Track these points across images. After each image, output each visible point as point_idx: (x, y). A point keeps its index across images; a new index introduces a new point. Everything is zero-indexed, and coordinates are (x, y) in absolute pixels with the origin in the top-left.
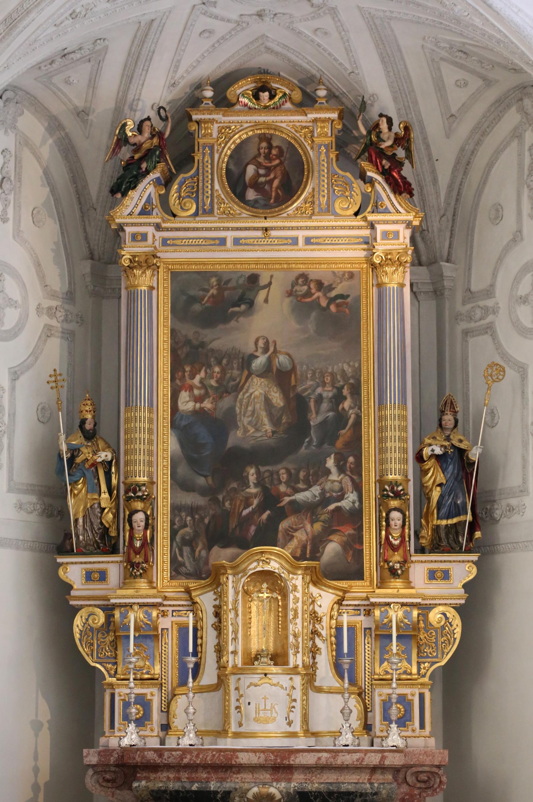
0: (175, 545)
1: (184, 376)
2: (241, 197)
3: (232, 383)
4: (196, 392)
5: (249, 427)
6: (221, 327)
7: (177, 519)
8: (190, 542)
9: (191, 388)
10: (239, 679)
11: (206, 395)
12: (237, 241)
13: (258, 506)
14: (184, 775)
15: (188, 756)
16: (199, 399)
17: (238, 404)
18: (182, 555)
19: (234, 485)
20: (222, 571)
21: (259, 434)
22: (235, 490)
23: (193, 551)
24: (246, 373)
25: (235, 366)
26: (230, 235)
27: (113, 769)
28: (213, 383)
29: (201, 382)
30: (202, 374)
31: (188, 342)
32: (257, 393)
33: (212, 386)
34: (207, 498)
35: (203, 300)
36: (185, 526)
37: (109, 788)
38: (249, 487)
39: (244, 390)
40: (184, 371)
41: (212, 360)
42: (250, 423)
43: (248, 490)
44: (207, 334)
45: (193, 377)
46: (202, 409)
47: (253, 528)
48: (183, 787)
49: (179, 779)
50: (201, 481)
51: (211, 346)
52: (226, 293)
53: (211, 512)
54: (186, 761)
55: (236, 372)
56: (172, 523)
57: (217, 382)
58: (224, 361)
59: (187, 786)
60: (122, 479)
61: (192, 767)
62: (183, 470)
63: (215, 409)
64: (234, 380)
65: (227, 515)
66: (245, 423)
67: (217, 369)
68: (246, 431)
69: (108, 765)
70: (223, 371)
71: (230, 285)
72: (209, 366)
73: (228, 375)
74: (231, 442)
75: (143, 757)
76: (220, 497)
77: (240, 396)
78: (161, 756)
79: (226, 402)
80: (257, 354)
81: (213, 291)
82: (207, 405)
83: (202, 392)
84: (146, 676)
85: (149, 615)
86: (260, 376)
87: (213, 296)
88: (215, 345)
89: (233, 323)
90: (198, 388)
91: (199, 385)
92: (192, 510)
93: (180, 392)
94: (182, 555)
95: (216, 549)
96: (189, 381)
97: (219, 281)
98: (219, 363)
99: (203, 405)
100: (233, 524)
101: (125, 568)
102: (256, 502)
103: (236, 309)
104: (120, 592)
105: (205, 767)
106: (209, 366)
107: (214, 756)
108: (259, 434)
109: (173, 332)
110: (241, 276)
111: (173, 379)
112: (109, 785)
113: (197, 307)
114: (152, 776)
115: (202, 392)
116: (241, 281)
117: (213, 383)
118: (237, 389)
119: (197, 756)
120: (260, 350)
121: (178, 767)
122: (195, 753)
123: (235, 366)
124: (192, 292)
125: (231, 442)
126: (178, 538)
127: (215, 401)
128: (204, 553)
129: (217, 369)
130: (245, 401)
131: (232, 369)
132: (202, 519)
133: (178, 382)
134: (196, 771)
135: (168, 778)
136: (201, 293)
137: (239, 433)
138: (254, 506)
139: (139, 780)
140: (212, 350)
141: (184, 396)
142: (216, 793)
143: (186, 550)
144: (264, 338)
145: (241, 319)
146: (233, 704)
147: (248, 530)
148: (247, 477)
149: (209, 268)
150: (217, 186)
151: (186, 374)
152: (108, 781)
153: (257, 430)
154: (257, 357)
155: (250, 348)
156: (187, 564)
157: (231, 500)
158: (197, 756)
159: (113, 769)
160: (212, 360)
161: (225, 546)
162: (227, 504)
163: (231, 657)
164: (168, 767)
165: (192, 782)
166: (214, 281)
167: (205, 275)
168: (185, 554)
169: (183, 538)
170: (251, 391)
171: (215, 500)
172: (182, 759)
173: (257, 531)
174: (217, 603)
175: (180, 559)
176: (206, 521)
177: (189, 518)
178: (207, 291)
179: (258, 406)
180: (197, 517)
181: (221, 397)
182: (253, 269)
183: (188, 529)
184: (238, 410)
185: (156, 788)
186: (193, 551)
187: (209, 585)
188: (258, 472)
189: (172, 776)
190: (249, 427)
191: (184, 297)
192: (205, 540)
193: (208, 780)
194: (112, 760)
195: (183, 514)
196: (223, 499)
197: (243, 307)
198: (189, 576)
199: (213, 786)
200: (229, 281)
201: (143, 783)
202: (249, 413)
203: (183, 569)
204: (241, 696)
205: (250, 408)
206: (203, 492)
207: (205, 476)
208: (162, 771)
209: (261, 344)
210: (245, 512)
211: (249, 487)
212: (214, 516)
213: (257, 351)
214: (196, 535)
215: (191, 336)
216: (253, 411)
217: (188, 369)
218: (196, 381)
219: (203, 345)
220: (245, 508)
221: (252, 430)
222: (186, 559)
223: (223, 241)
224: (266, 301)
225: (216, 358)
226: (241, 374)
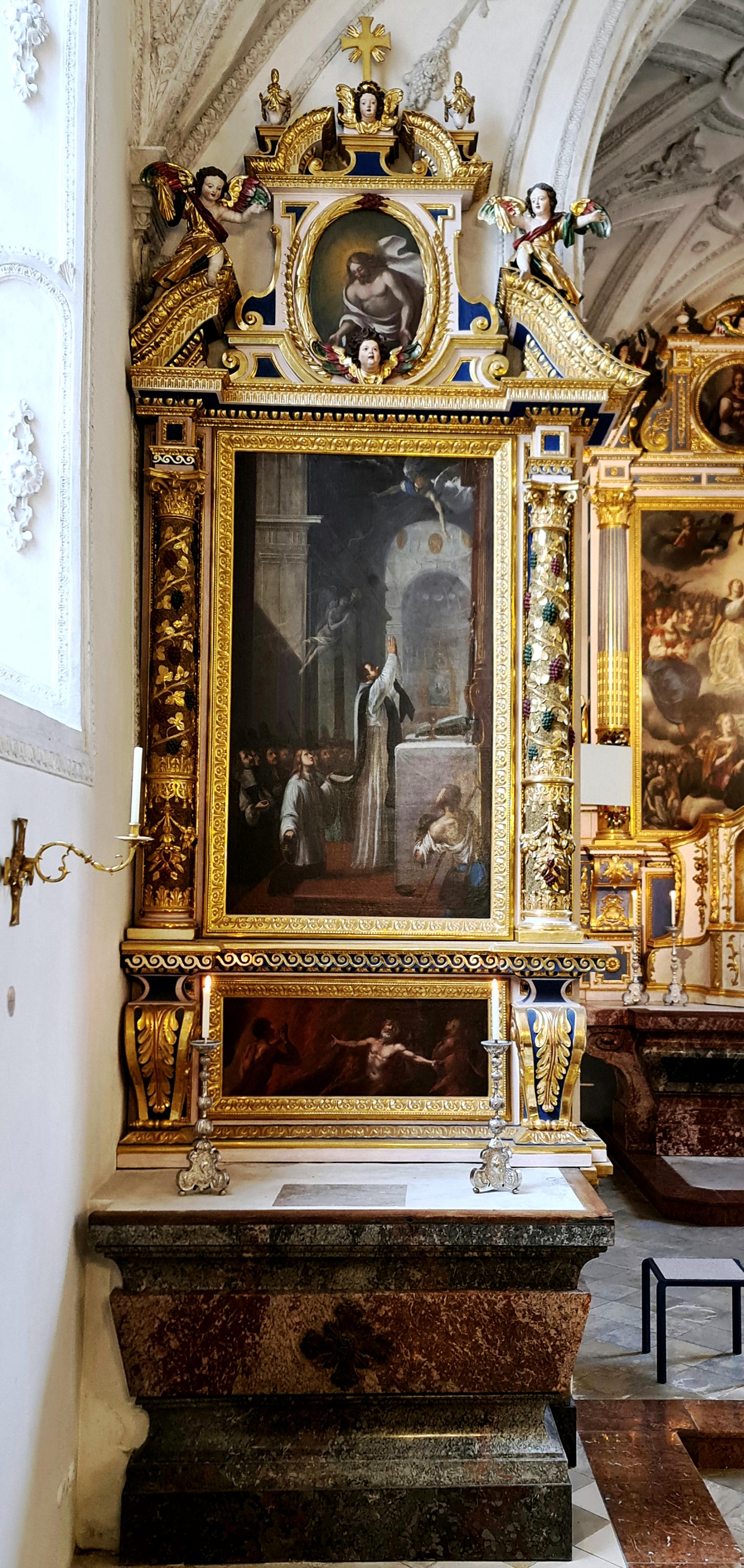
0: (646, 794)
1: (655, 620)
2: (714, 433)
3: (705, 628)
4: (668, 637)
5: (723, 674)
6: (694, 569)
7: (649, 768)
8: (662, 792)
9: (662, 633)
10: (733, 936)
11: (679, 640)
12: (711, 479)
13: (732, 755)
14: (697, 1042)
15: (705, 1023)
16: (671, 645)
17: (711, 651)
18: (654, 805)
19: (708, 733)
20: (711, 823)
21: (731, 682)
22: (707, 738)
23: (665, 801)
24: (719, 618)
25: (708, 610)
26: (704, 472)
27: (611, 1030)
28: (685, 627)
29: (673, 626)
30: (674, 618)
31: (660, 585)
32: (730, 639)
33: (684, 632)
34: (679, 747)
35: (674, 540)
36: (657, 775)
37: (606, 1050)
38: (722, 735)
39: (718, 635)
40: (655, 615)
41: (684, 603)
42: (723, 669)
43: (721, 739)
44: (679, 577)
45: (664, 621)
46: (674, 654)
47: (727, 778)
48: (698, 1055)
49: (690, 1046)
50: (673, 729)
51: (683, 589)
52: (699, 534)
53: (684, 761)
54: (701, 1027)
55: (709, 617)
56: (644, 772)
57: (689, 626)
58: (697, 605)
59: (702, 1053)
60: (594, 726)
61: (707, 1034)
62: (655, 717)
63: (687, 655)
64: (708, 625)
65: (700, 763)
66: (719, 670)
67: (689, 613)
68: (719, 678)
69: (607, 1026)
70: (696, 616)
71: (703, 525)
72: (682, 610)
73: (701, 620)
74: (704, 689)
75: (656, 1023)
76: (693, 746)
77: (714, 641)
78: (675, 1022)
79: (699, 648)
80: (731, 598)
81: (685, 532)
82: (679, 650)
83: (674, 637)
84: (620, 928)
85: (631, 868)
86: (734, 620)
87: (685, 536)
88: (688, 588)
89: (706, 566)
90: (671, 633)
91: (671, 630)
92: (664, 759)
93: (651, 636)
94: (654, 805)
95: (688, 798)
96: (660, 626)
97: (692, 521)
98: (692, 607)
99: (675, 650)
100: (706, 773)
101: (599, 817)
102: (729, 751)
103: (709, 551)
104: (597, 843)
105: (721, 1034)
106: (682, 610)
107: (732, 1023)
108: (731, 682)
109: (644, 573)
110: (714, 517)
111: (644, 623)
112: (608, 1047)
113: (668, 548)
114: (663, 1042)
115: (674, 637)
116: (715, 521)
117: (685, 627)
118: (709, 634)
119: (714, 1023)
120: (734, 594)
121: (690, 1034)
122: (711, 1020)
123: (708, 610)
124: (663, 533)
125: (704, 689)
126: (650, 787)
127: (687, 647)
128: (676, 803)
129: (689, 613)
130: (718, 648)
131: (705, 613)
132: (674, 768)
133: (649, 626)
134: (710, 1038)
135: (680, 1044)
136: (673, 533)
137: (713, 680)
138: (727, 756)
139: (650, 1046)
140: (685, 594)
141: (655, 640)
142: (731, 1061)
143: (658, 799)
144: (739, 581)
145: (715, 561)
146: (725, 961)
147: (722, 780)
148: (720, 726)
149: (680, 507)
150: (692, 420)
151: (658, 618)
152: (606, 1043)
153: (731, 677)
154: (730, 601)
155: (723, 592)
156: (659, 813)
157: (705, 749)
158: (714, 1023)
159: (611, 1030)
160: (684, 603)
161: (698, 796)
162: (700, 753)
163: (723, 913)
164: (679, 1034)
165: (708, 1050)
166: (686, 520)
167: (676, 516)
168: (657, 803)
169: (655, 787)
170: (724, 636)
171: (687, 749)
172: (698, 1026)
173: (730, 781)
174: (699, 855)
175: (652, 808)
176: (679, 770)
177: (661, 767)
178: (680, 531)
179: (732, 653)
180: (669, 765)
181: (693, 643)
182: (728, 507)
183: (659, 778)
184: (711, 656)
185: (668, 1055)
186: (665, 801)
187: (690, 837)
188: (733, 721)
189: (683, 1042)
190: (723, 674)
191: (655, 538)
192: (678, 790)
193: (722, 1048)
194: (611, 1021)
195: (655, 763)
196: (697, 746)
197: (717, 549)
198: (661, 826)
199: (728, 1053)
200: (701, 521)
201: (655, 1050)
202: (722, 659)
203: (655, 819)
204: (735, 954)
205: (724, 654)
206: (675, 740)
207: (678, 724)
208: (673, 1038)
209: (735, 587)
210: (719, 762)
211: (722, 735)
212: (686, 765)
213: (730, 594)
214: (669, 784)
215: (662, 579)
216: (727, 657)
217: (659, 612)
218: (668, 625)
219: (674, 588)
220: (718, 758)
221: (726, 677)
222: (657, 808)
223: (698, 479)
224: (741, 542)
225: (689, 602)
226: (714, 620)
